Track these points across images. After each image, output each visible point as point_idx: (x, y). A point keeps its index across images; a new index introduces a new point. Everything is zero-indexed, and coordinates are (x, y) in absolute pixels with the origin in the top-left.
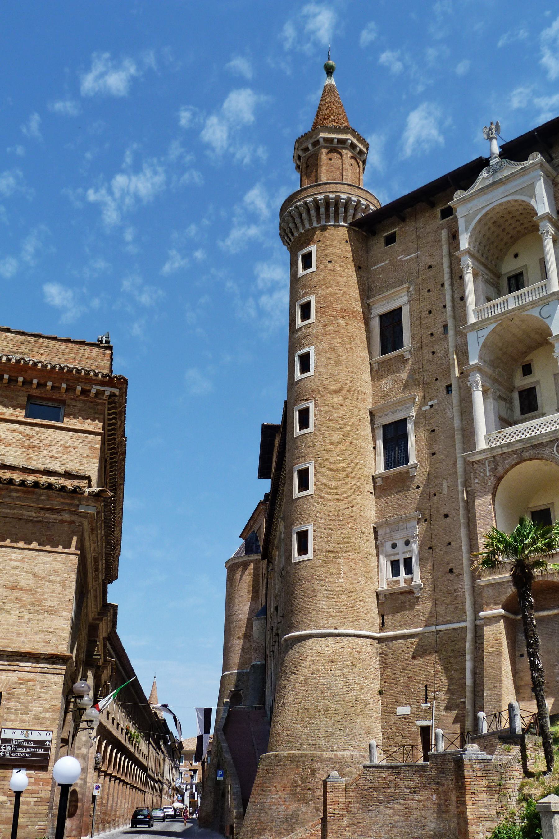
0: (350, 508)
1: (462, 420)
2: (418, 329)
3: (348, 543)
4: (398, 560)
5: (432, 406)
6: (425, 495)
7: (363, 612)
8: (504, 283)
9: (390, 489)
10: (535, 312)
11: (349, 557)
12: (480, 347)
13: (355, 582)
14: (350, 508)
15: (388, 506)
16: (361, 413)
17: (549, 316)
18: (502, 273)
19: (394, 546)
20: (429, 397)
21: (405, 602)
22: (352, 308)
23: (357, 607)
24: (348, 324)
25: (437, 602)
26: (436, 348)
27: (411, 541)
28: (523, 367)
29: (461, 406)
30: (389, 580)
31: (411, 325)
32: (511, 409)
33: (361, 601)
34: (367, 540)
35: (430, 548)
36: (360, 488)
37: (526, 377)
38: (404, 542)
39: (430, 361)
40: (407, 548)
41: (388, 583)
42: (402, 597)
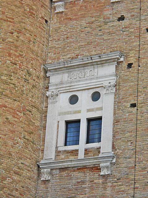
0: (15, 34)
3: (6, 83)
4: (78, 121)
6: (133, 30)
7: (17, 190)
9: (76, 19)
11: (6, 104)
13: (10, 143)
14: (15, 34)
15: (71, 42)
19: (74, 100)
21: (83, 182)
23: (9, 180)
25: (137, 185)
27: (102, 92)
30: (60, 149)
33: (16, 173)
34: (33, 86)
35: (133, 105)
36: (33, 9)
38: (90, 95)
40: (97, 104)
41: (58, 153)
42: (79, 175)
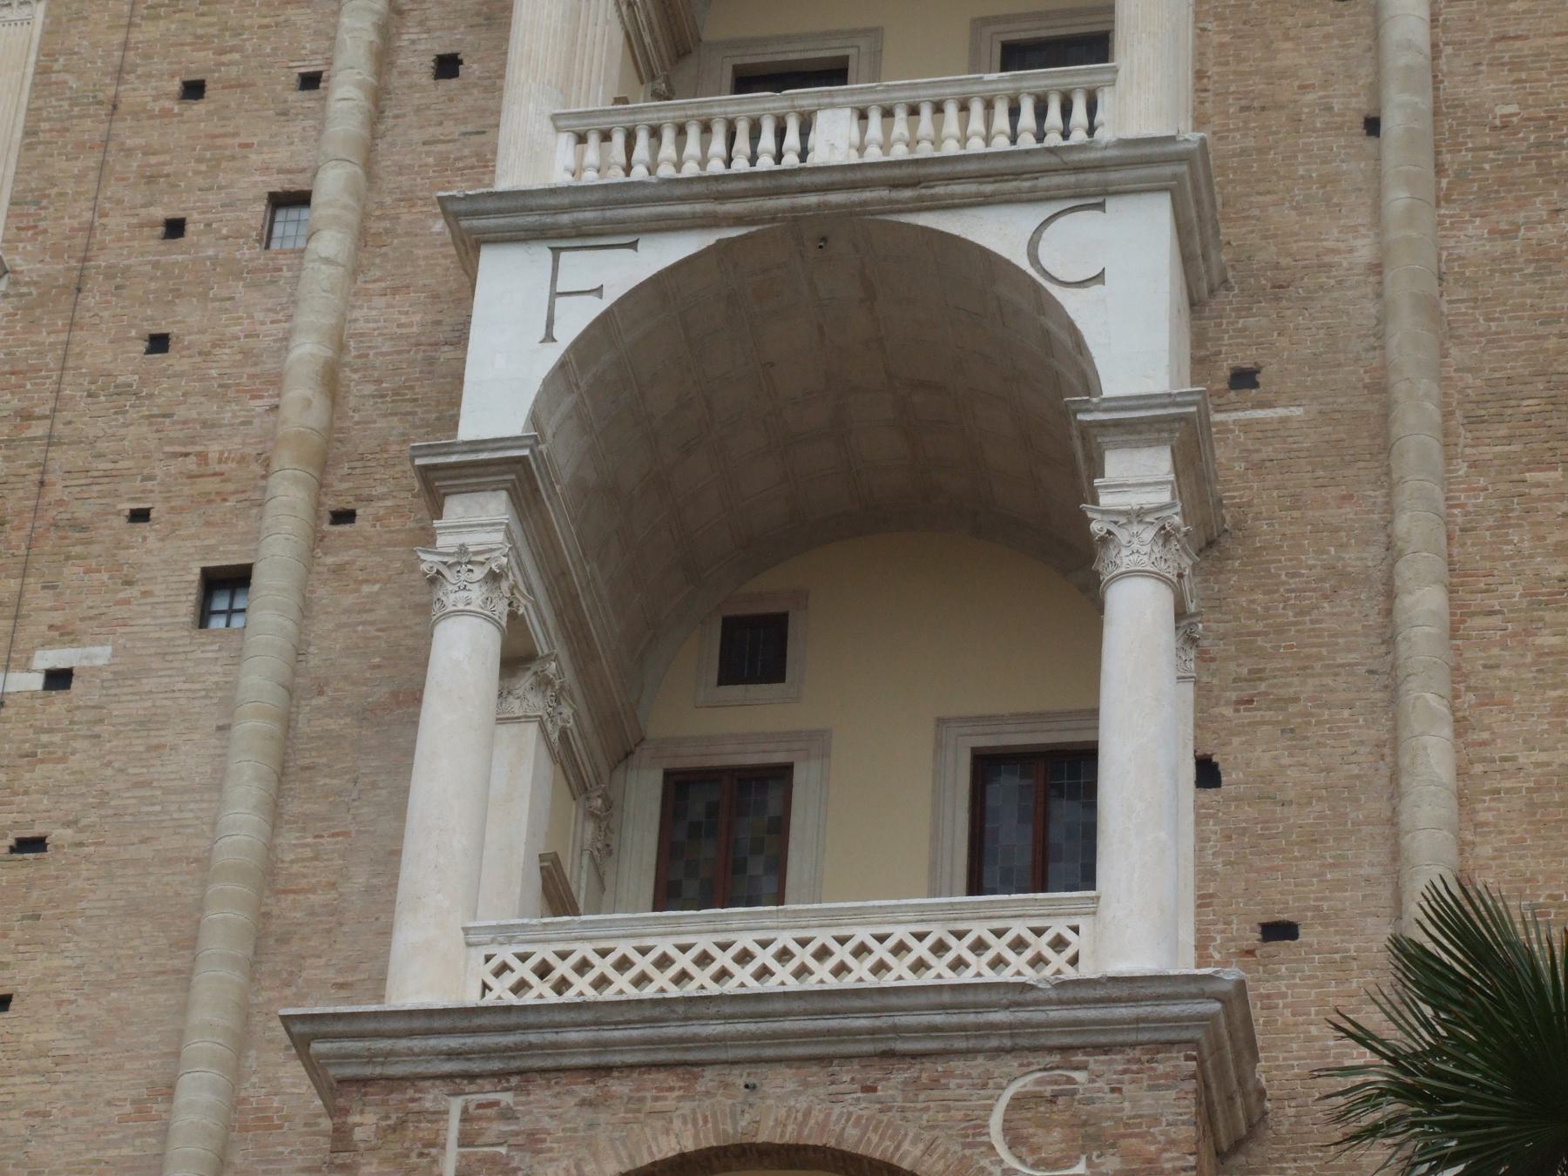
1: (275, 813)
2: (76, 167)
5: (58, 679)
8: (728, 78)
10: (1000, 232)
12: (552, 356)
17: (1099, 278)
18: (706, 36)
20: (58, 618)
26: (184, 320)
28: (734, 629)
29: (288, 723)
31: (29, 132)
32: (604, 854)
37: (736, 692)
39: (123, 390)
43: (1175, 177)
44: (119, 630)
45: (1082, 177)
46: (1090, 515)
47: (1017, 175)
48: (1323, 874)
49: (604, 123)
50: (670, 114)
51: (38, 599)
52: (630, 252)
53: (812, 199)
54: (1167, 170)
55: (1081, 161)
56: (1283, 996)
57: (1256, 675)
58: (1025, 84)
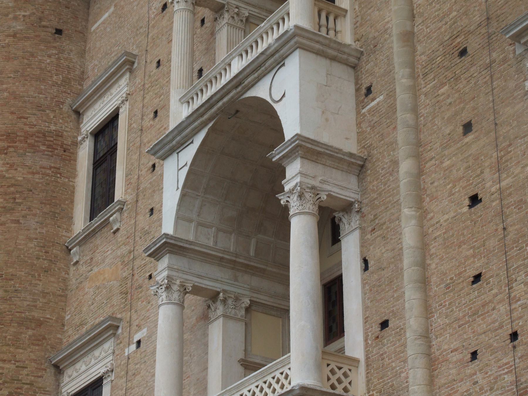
16: (25, 372)
17: (284, 96)
22: (27, 128)
24: (12, 166)
31: (128, 149)
43: (296, 43)
44: (148, 321)
45: (275, 57)
46: (280, 198)
47: (260, 66)
48: (393, 296)
49: (190, 95)
50: (202, 84)
51: (134, 317)
52: (192, 145)
53: (220, 104)
54: (292, 42)
55: (271, 53)
56: (386, 353)
57: (376, 217)
58: (271, 22)
